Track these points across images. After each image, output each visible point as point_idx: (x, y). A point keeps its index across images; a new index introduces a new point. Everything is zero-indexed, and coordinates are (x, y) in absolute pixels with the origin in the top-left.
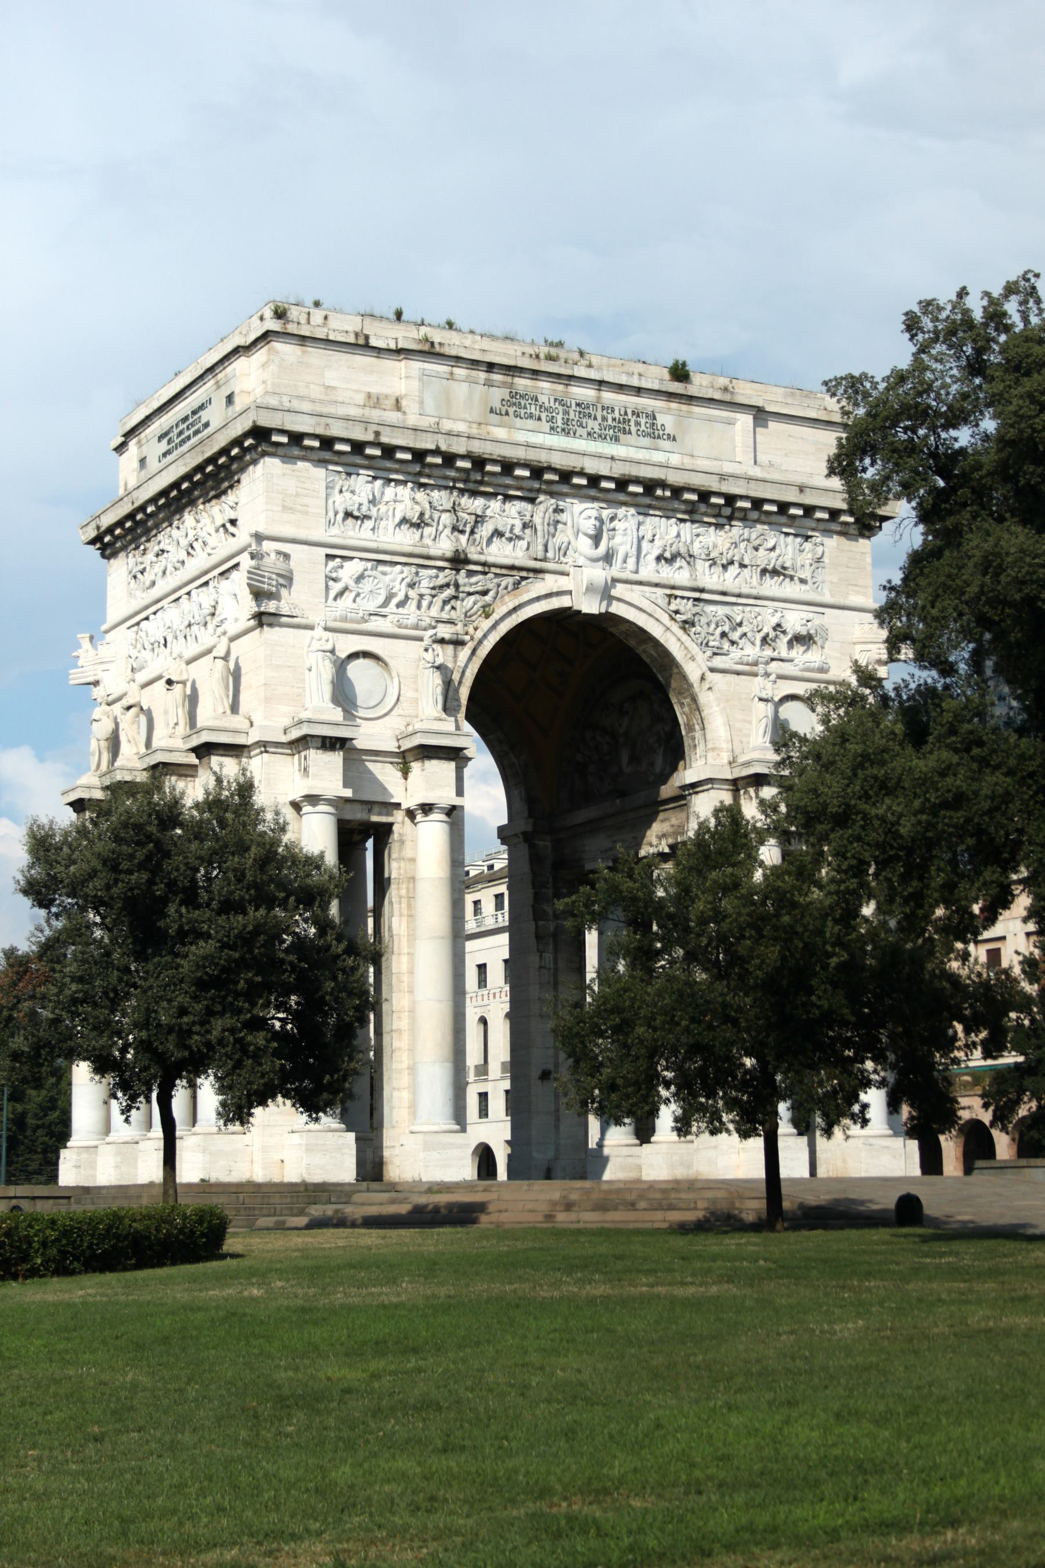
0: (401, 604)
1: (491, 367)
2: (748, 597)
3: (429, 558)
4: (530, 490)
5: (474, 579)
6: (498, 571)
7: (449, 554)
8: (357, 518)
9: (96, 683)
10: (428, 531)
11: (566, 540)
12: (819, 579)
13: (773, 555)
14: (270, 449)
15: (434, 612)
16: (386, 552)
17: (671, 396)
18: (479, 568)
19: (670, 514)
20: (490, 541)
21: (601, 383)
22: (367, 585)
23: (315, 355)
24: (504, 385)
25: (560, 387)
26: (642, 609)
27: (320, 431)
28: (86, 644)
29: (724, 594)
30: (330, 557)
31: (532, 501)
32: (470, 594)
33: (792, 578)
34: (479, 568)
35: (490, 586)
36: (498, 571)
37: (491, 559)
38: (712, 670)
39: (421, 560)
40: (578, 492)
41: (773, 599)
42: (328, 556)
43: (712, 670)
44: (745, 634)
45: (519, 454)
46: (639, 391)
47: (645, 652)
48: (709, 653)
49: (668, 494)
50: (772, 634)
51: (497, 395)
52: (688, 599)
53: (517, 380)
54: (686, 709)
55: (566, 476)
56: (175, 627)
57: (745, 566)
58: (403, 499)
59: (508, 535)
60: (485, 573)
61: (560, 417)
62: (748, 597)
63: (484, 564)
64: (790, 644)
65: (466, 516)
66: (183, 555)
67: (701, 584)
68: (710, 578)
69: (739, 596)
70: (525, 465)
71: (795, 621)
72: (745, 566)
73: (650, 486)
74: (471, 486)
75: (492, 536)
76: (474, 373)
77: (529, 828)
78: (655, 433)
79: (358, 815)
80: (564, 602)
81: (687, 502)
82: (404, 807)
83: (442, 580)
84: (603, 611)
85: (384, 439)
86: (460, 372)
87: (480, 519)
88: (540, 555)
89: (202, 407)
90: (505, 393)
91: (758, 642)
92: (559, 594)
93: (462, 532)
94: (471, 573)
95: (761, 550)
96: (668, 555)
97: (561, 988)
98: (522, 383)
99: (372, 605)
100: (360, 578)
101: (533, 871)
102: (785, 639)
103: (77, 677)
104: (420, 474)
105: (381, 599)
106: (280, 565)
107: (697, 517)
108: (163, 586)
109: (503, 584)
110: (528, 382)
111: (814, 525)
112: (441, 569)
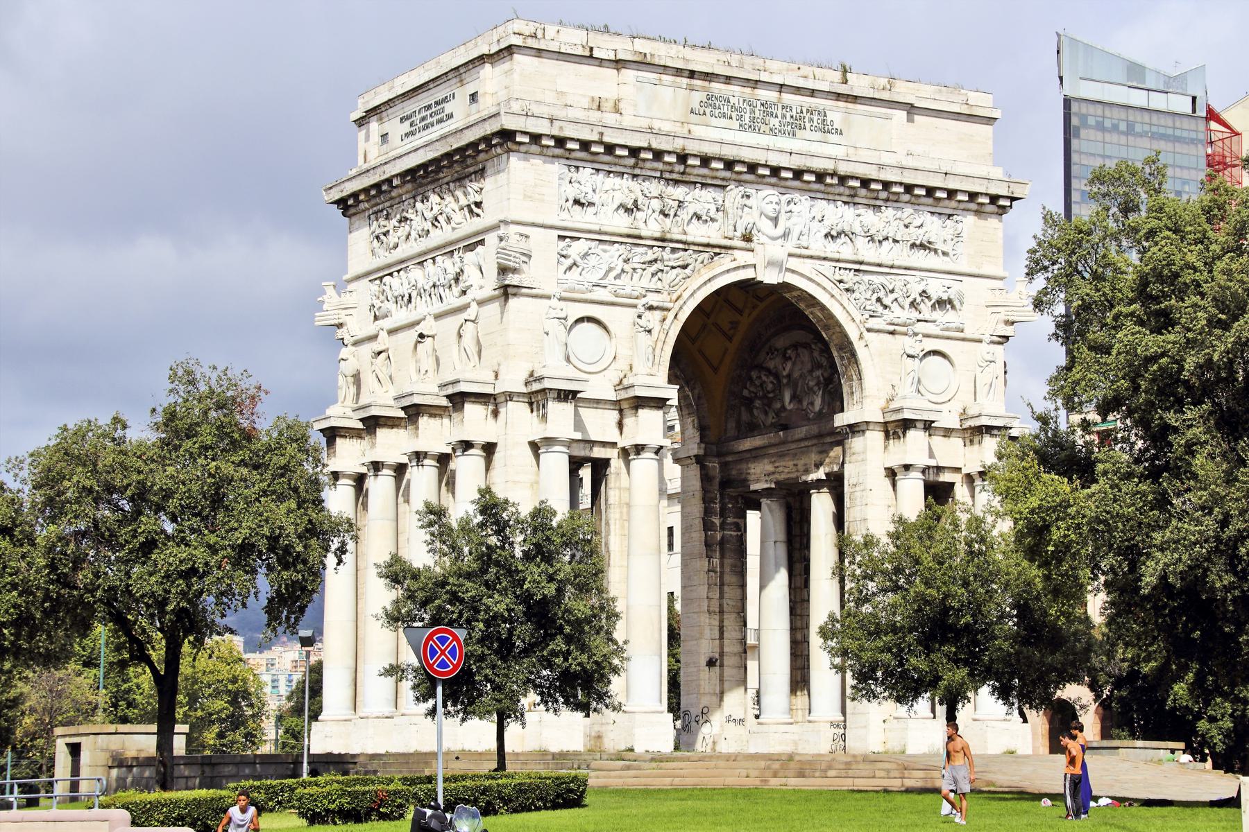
0: (617, 277)
1: (692, 74)
2: (899, 268)
3: (640, 237)
4: (723, 179)
5: (677, 255)
6: (696, 248)
7: (658, 235)
8: (582, 205)
9: (340, 326)
10: (639, 215)
11: (752, 221)
12: (959, 251)
13: (921, 231)
14: (515, 147)
16: (606, 233)
17: (839, 96)
19: (837, 198)
22: (592, 260)
23: (548, 64)
24: (704, 89)
25: (748, 90)
27: (556, 132)
28: (331, 291)
29: (880, 265)
30: (562, 238)
32: (673, 268)
33: (936, 251)
35: (689, 261)
37: (690, 239)
38: (869, 330)
39: (635, 238)
43: (869, 330)
46: (812, 93)
47: (812, 314)
50: (919, 299)
53: (714, 85)
54: (846, 362)
55: (752, 167)
56: (419, 285)
58: (622, 188)
59: (704, 218)
61: (747, 116)
62: (899, 268)
63: (685, 243)
64: (933, 306)
65: (671, 202)
66: (428, 225)
67: (861, 259)
69: (892, 267)
71: (936, 288)
73: (821, 176)
74: (675, 176)
76: (679, 79)
77: (702, 452)
78: (825, 128)
79: (580, 452)
80: (748, 274)
81: (850, 188)
82: (620, 445)
83: (650, 256)
85: (606, 139)
86: (667, 78)
88: (731, 234)
89: (446, 100)
90: (702, 96)
91: (907, 306)
93: (666, 215)
94: (674, 250)
97: (726, 588)
98: (716, 87)
99: (595, 280)
100: (585, 255)
101: (703, 488)
103: (322, 319)
104: (633, 167)
106: (523, 245)
107: (857, 200)
108: (405, 250)
109: (700, 259)
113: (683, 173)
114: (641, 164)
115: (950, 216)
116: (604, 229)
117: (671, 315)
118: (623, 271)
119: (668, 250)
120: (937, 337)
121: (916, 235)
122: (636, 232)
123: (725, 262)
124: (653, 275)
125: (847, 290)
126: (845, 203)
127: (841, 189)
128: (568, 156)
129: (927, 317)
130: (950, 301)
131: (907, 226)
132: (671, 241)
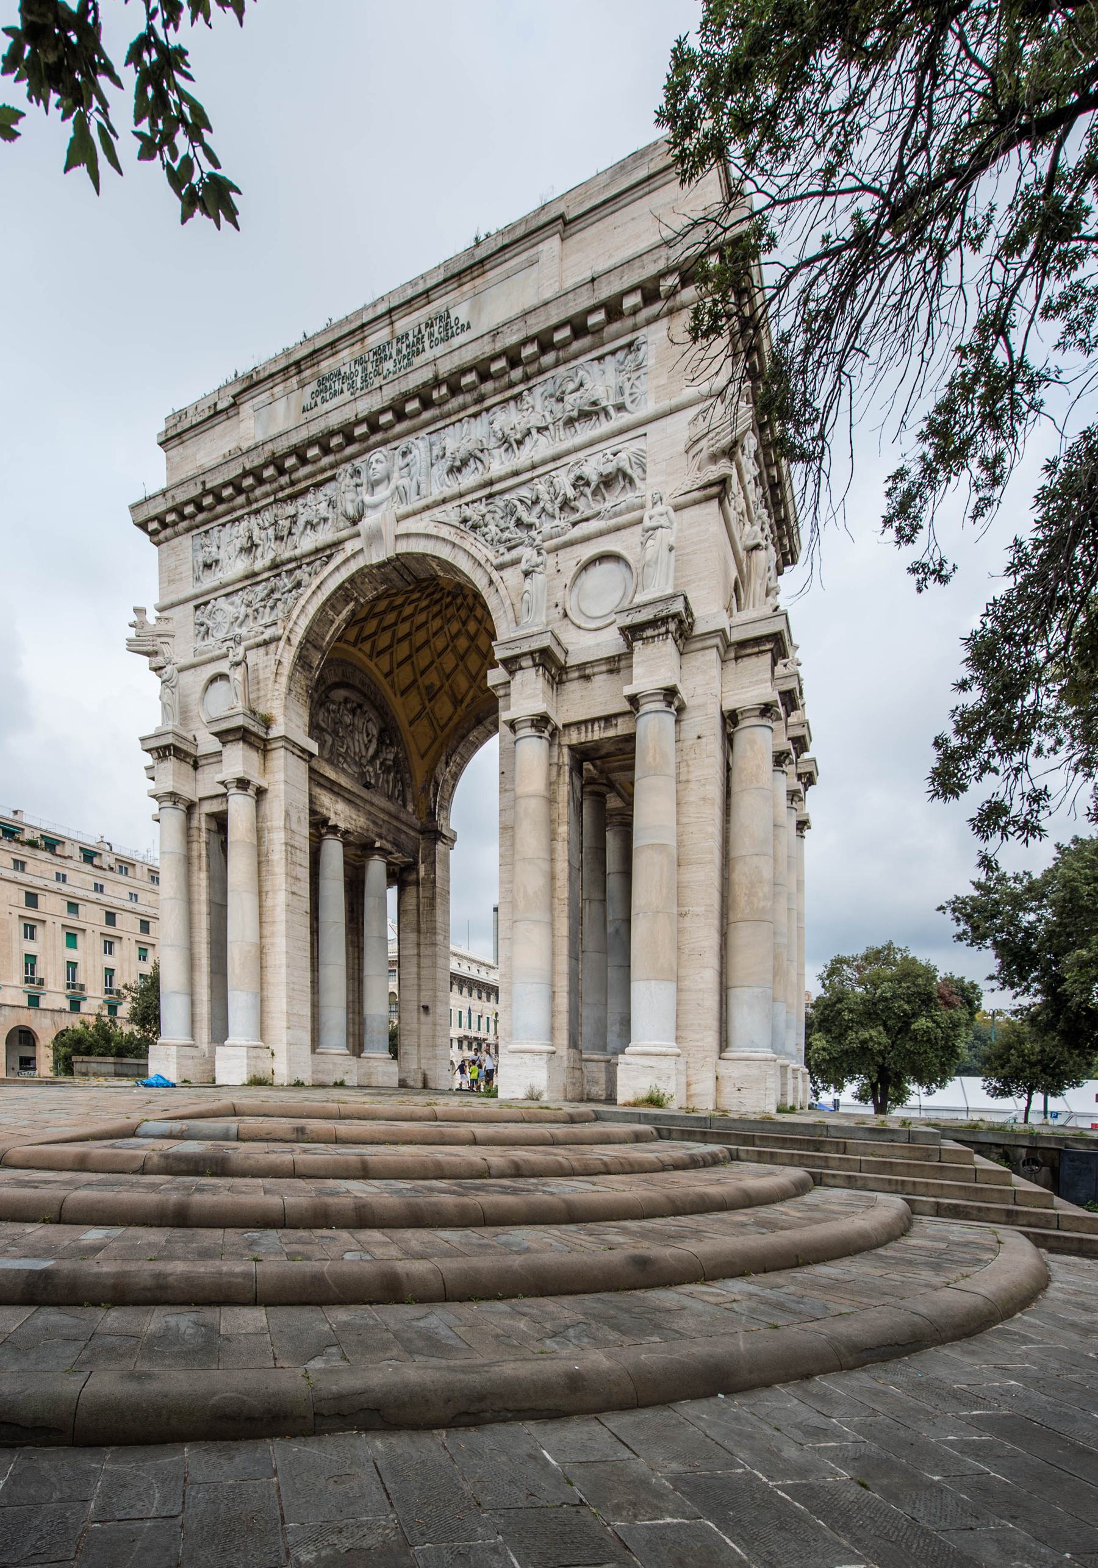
2: (544, 463)
20: (303, 533)
26: (435, 537)
27: (170, 504)
29: (516, 473)
32: (290, 591)
36: (308, 560)
37: (298, 552)
38: (500, 567)
41: (577, 450)
42: (197, 607)
44: (543, 510)
48: (502, 550)
50: (571, 493)
52: (480, 499)
57: (546, 428)
60: (300, 567)
62: (544, 463)
63: (296, 559)
67: (487, 476)
69: (534, 467)
72: (546, 428)
74: (287, 491)
75: (305, 528)
84: (391, 554)
85: (208, 486)
94: (290, 572)
95: (566, 398)
96: (458, 463)
99: (220, 635)
102: (588, 491)
105: (227, 626)
107: (488, 403)
112: (268, 579)
115: (630, 345)
118: (247, 616)
124: (272, 608)
125: (474, 527)
126: (475, 416)
127: (460, 400)
129: (588, 513)
130: (625, 475)
132: (283, 564)
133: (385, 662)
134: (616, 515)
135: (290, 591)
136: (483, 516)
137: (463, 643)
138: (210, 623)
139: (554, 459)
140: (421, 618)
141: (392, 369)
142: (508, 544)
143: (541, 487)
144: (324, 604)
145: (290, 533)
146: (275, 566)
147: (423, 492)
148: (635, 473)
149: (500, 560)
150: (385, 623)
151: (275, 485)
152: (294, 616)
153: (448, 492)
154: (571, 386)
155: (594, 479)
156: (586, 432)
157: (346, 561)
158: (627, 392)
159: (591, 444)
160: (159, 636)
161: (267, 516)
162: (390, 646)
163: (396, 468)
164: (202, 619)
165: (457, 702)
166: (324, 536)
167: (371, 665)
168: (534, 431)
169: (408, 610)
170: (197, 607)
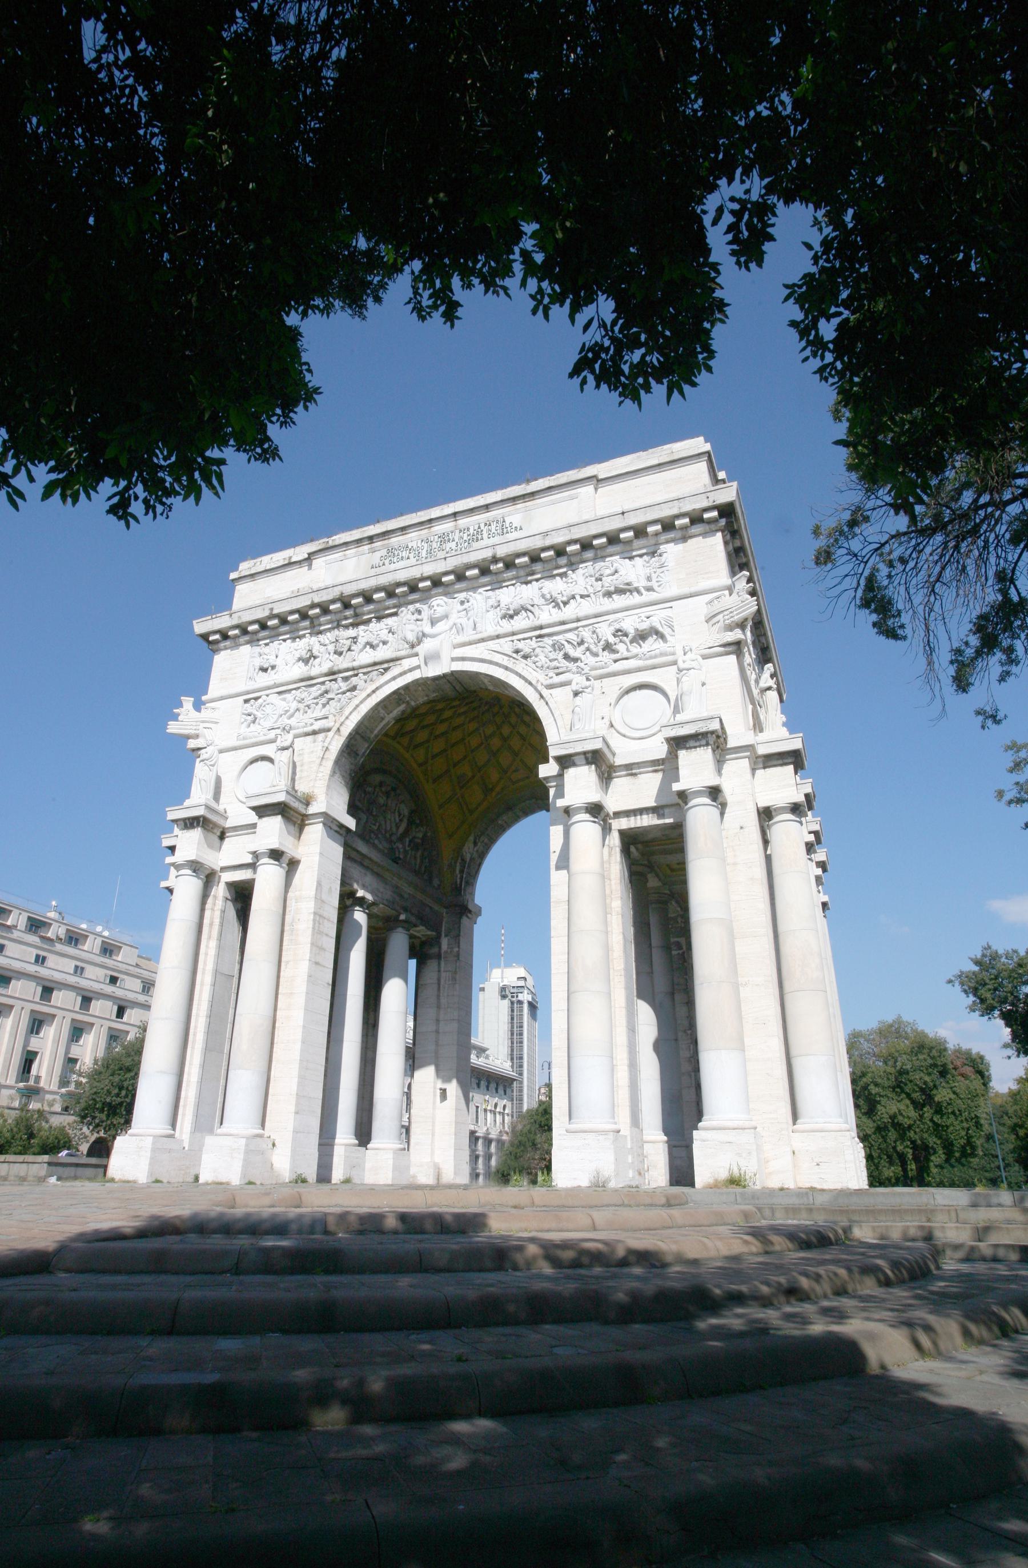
1: (371, 539)
2: (587, 618)
3: (312, 678)
4: (394, 607)
6: (365, 670)
10: (318, 660)
13: (614, 577)
15: (314, 715)
16: (282, 685)
18: (350, 673)
20: (361, 650)
21: (455, 514)
22: (268, 709)
23: (261, 583)
29: (563, 623)
31: (395, 614)
32: (344, 693)
34: (350, 673)
36: (365, 670)
37: (355, 664)
40: (426, 596)
41: (615, 612)
42: (246, 701)
44: (588, 649)
45: (372, 583)
49: (501, 565)
51: (376, 557)
52: (531, 638)
55: (413, 587)
57: (588, 596)
60: (356, 675)
62: (587, 618)
63: (353, 669)
67: (537, 623)
68: (547, 615)
69: (578, 620)
70: (378, 589)
72: (588, 596)
83: (323, 688)
85: (275, 612)
86: (351, 552)
87: (355, 640)
90: (384, 552)
92: (411, 670)
93: (340, 654)
96: (511, 612)
98: (395, 541)
99: (268, 724)
105: (275, 717)
110: (401, 538)
111: (652, 541)
112: (323, 683)
113: (356, 615)
114: (316, 622)
116: (278, 681)
117: (331, 734)
118: (298, 710)
119: (340, 680)
120: (639, 670)
121: (609, 583)
122: (306, 675)
123: (395, 671)
124: (324, 706)
125: (525, 657)
128: (253, 640)
129: (626, 654)
130: (657, 633)
131: (601, 580)
132: (340, 672)
133: (421, 754)
134: (651, 658)
135: (344, 693)
136: (534, 650)
137: (496, 742)
138: (259, 714)
139: (596, 616)
140: (458, 721)
141: (454, 547)
142: (557, 671)
143: (586, 634)
144: (378, 704)
145: (349, 650)
146: (332, 673)
147: (479, 629)
148: (666, 631)
149: (549, 682)
150: (425, 723)
151: (338, 616)
152: (347, 712)
153: (500, 631)
154: (608, 572)
155: (632, 632)
156: (619, 601)
157: (401, 674)
158: (654, 579)
159: (627, 609)
160: (203, 722)
161: (329, 637)
162: (428, 741)
163: (455, 611)
164: (249, 711)
165: (487, 790)
166: (382, 653)
167: (407, 755)
168: (578, 597)
169: (447, 714)
170: (246, 701)
